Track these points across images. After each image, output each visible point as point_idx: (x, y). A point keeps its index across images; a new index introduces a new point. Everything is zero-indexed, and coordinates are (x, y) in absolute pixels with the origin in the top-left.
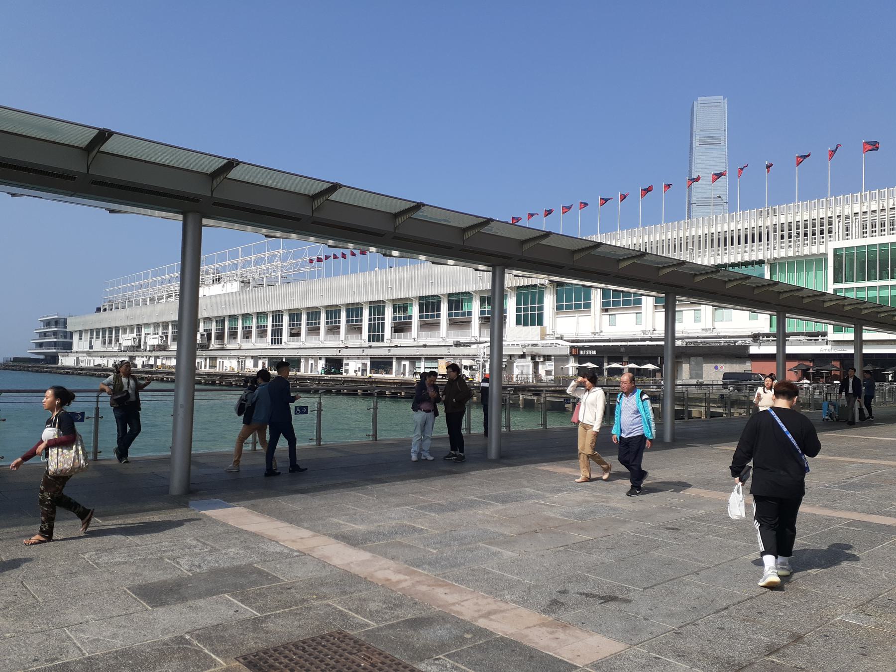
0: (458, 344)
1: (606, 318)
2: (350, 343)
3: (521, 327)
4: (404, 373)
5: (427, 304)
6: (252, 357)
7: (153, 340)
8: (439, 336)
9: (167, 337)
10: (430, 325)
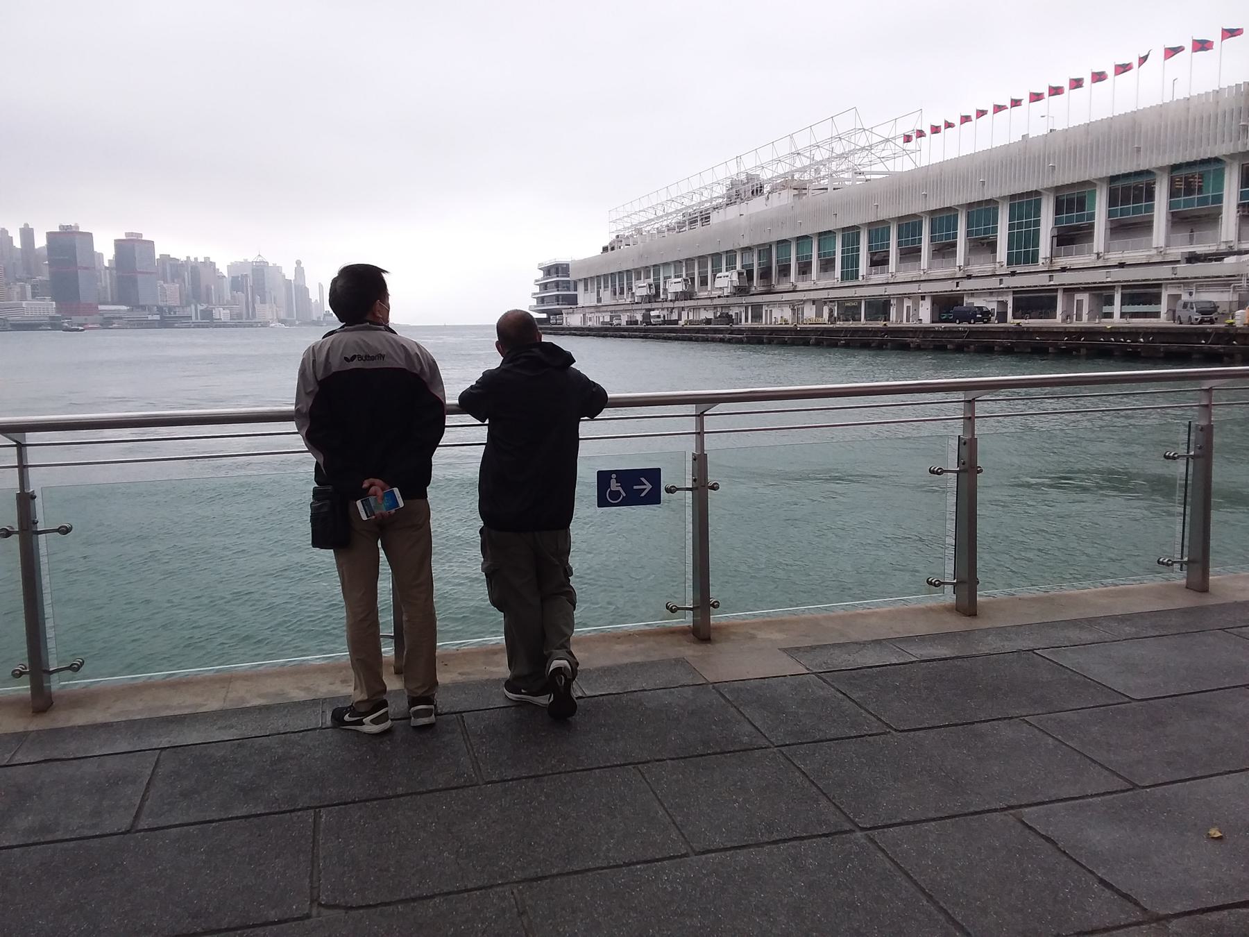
0: (1192, 258)
2: (975, 269)
4: (1079, 318)
5: (1126, 189)
6: (814, 302)
7: (675, 286)
9: (693, 280)
10: (1129, 226)
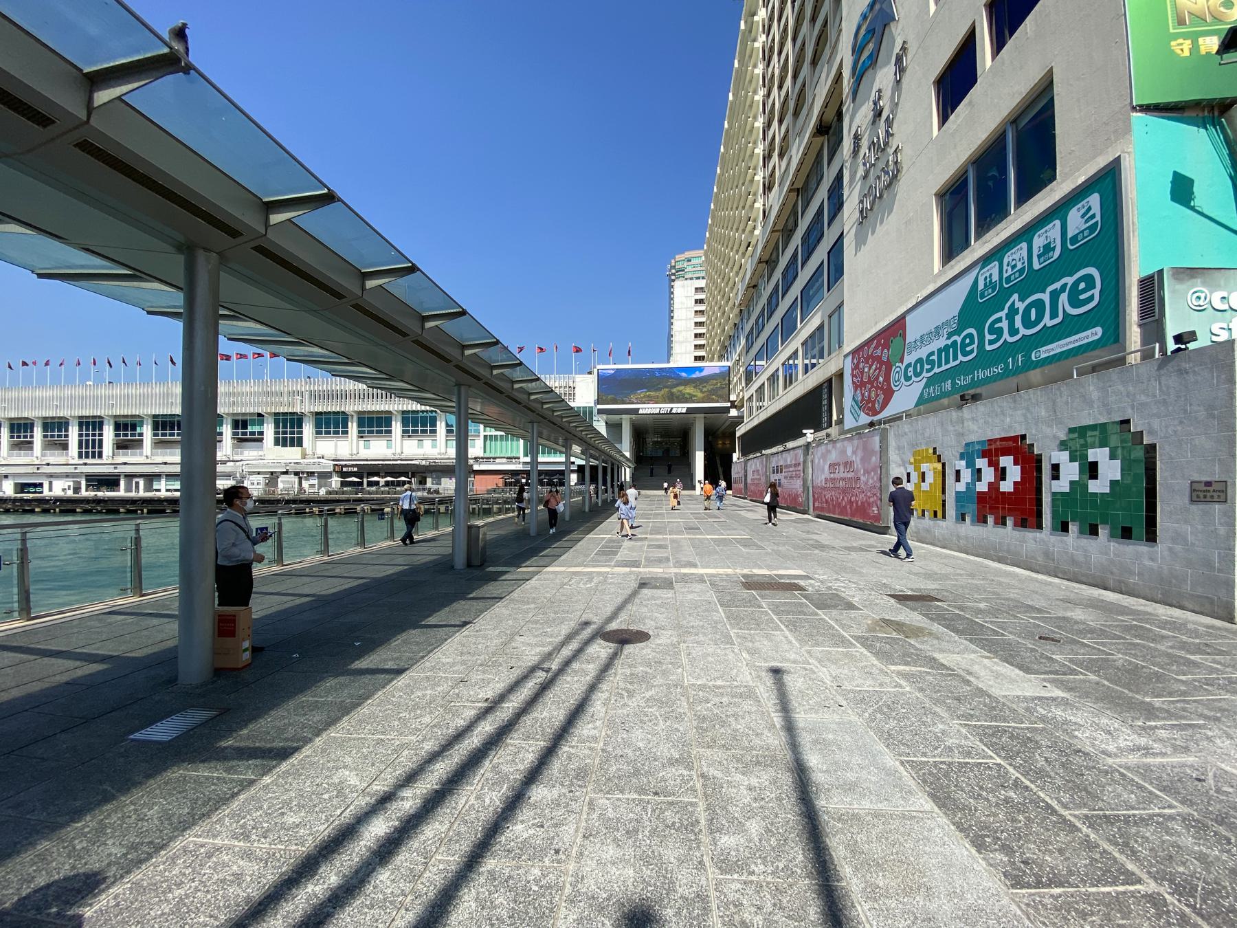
1: (362, 443)
3: (279, 448)
8: (141, 454)
